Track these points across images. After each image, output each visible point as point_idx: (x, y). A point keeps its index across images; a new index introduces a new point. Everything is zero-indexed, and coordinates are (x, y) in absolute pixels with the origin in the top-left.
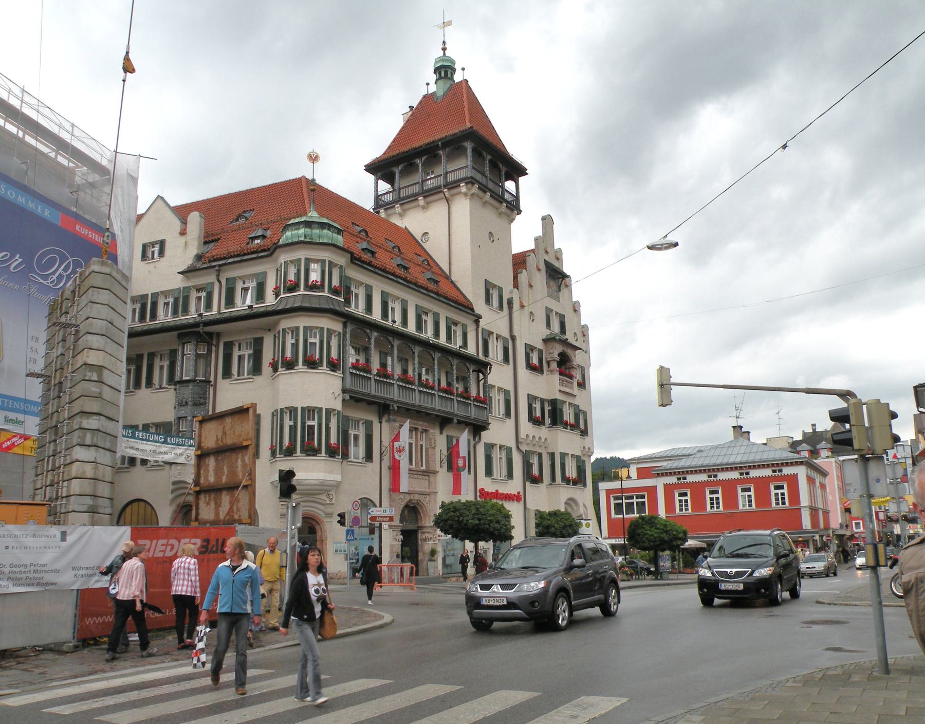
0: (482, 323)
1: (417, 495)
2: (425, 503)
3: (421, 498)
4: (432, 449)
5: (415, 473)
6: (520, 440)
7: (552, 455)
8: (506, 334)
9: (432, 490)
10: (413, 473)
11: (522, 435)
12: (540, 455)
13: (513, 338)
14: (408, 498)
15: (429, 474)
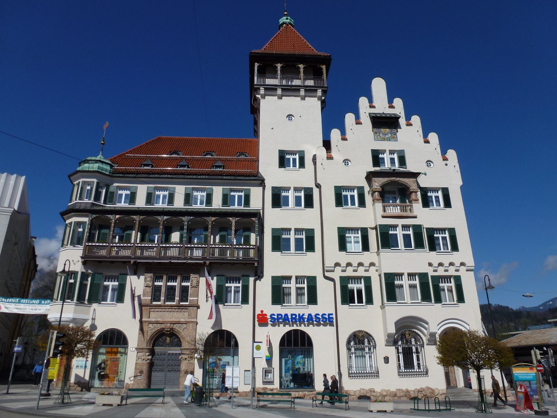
0: (269, 185)
1: (169, 325)
2: (181, 330)
3: (176, 327)
4: (194, 288)
5: (168, 307)
6: (326, 269)
7: (380, 276)
8: (312, 185)
9: (189, 320)
10: (166, 307)
11: (329, 263)
12: (368, 280)
13: (318, 186)
14: (159, 327)
15: (187, 308)
